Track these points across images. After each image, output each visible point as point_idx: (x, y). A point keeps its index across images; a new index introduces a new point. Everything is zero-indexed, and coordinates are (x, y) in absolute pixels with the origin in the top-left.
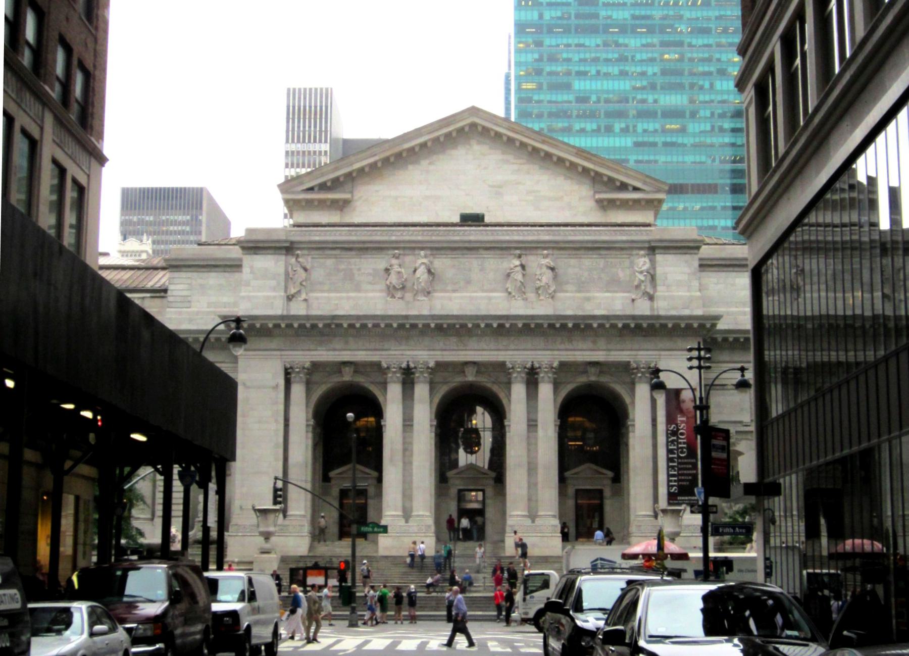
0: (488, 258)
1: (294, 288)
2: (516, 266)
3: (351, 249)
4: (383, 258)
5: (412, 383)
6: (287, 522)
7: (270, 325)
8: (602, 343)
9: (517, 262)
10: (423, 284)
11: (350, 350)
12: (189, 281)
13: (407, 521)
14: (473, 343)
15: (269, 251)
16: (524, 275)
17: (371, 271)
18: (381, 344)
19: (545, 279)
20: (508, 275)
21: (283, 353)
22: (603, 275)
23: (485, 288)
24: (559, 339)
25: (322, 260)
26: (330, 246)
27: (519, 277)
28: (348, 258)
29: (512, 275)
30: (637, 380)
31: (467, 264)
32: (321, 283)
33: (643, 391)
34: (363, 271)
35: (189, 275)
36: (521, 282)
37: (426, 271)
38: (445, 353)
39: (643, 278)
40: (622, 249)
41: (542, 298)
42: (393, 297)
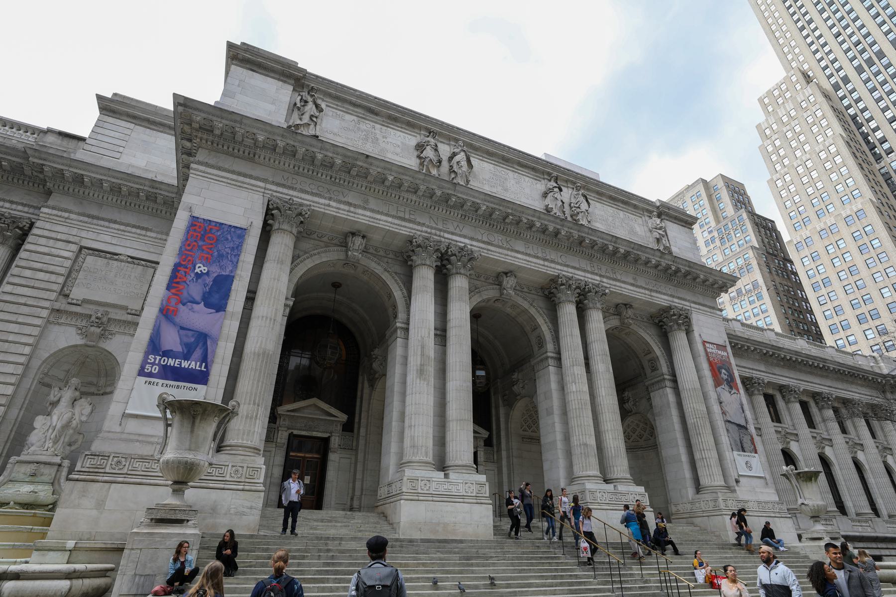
1: (301, 119)
2: (556, 187)
3: (376, 114)
4: (416, 137)
6: (222, 458)
7: (261, 138)
8: (641, 282)
9: (556, 185)
11: (373, 211)
12: (128, 132)
13: (446, 476)
15: (272, 75)
17: (399, 144)
18: (412, 217)
20: (545, 195)
21: (269, 186)
22: (624, 225)
24: (604, 268)
25: (339, 112)
26: (354, 99)
28: (373, 121)
31: (503, 172)
32: (335, 134)
33: (679, 340)
34: (389, 140)
35: (132, 126)
36: (562, 201)
37: (465, 159)
39: (660, 232)
40: (635, 207)
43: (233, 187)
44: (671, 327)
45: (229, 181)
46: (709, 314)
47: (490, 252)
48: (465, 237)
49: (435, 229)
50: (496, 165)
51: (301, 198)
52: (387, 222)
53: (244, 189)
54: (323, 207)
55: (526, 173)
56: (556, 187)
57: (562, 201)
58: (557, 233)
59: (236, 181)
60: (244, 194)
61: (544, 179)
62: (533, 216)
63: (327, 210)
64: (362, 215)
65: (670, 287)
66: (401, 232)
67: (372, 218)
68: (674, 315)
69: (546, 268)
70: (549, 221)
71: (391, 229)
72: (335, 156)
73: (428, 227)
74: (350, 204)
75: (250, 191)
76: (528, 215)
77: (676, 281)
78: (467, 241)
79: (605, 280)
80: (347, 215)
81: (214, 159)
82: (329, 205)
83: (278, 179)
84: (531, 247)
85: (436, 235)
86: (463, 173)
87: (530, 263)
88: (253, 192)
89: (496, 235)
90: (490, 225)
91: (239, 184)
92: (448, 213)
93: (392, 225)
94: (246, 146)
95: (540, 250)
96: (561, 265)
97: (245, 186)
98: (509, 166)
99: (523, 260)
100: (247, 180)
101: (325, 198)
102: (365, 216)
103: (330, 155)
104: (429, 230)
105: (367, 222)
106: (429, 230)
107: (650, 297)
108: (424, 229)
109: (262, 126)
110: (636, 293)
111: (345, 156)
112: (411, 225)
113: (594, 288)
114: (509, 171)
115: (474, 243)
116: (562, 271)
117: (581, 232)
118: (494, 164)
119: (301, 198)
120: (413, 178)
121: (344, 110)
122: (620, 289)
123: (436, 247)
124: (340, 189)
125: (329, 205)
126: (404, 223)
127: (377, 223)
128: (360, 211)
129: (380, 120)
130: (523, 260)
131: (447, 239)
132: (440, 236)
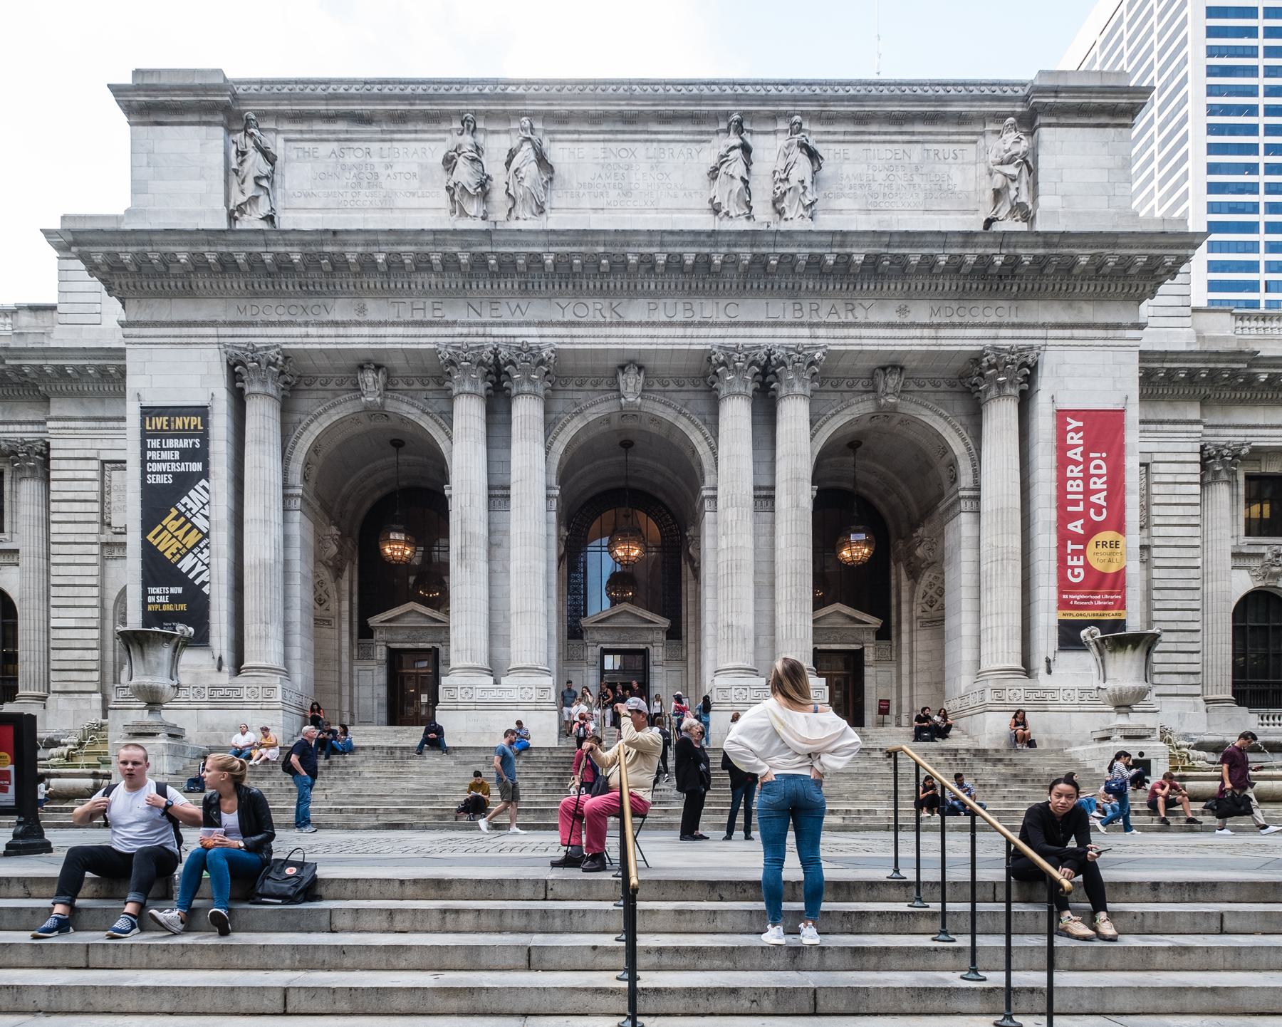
0: (668, 141)
2: (734, 148)
5: (509, 400)
8: (921, 312)
9: (736, 141)
10: (526, 183)
11: (371, 324)
14: (637, 310)
16: (748, 170)
18: (438, 313)
19: (795, 176)
20: (714, 173)
23: (662, 205)
24: (825, 306)
27: (738, 168)
29: (723, 169)
30: (993, 392)
36: (742, 179)
38: (576, 331)
41: (788, 215)
42: (464, 213)
43: (179, 346)
44: (986, 391)
45: (172, 340)
46: (1101, 342)
47: (576, 340)
48: (528, 324)
49: (476, 324)
50: (610, 141)
51: (267, 336)
52: (396, 336)
53: (193, 346)
54: (299, 340)
55: (677, 133)
56: (734, 148)
57: (742, 179)
58: (704, 264)
59: (181, 337)
60: (193, 353)
61: (717, 133)
62: (650, 244)
63: (306, 343)
64: (358, 336)
65: (1001, 303)
66: (421, 347)
67: (373, 336)
68: (994, 366)
69: (688, 341)
70: (683, 244)
71: (404, 346)
72: (289, 249)
73: (463, 324)
74: (335, 324)
75: (201, 346)
76: (640, 245)
77: (1015, 288)
78: (533, 331)
79: (821, 332)
80: (336, 343)
81: (147, 311)
82: (307, 336)
83: (233, 316)
84: (661, 306)
85: (477, 335)
86: (525, 194)
87: (655, 340)
88: (205, 346)
89: (590, 302)
90: (574, 286)
91: (185, 340)
92: (495, 286)
93: (405, 340)
94: (175, 276)
95: (680, 306)
96: (722, 325)
97: (193, 340)
98: (636, 132)
99: (640, 337)
100: (193, 331)
101: (299, 325)
102: (362, 336)
103: (282, 249)
104: (465, 330)
105: (366, 346)
106: (465, 330)
107: (934, 342)
108: (458, 330)
109: (177, 237)
110: (897, 342)
111: (303, 244)
112: (434, 330)
113: (790, 357)
114: (637, 145)
115: (547, 331)
116: (724, 337)
117: (758, 246)
118: (604, 141)
119: (267, 336)
120: (416, 244)
121: (314, 136)
122: (858, 341)
123: (477, 359)
124: (320, 301)
125: (307, 336)
126: (423, 331)
127: (381, 343)
128: (354, 330)
129: (376, 132)
130: (640, 337)
131: (498, 336)
132: (484, 336)
